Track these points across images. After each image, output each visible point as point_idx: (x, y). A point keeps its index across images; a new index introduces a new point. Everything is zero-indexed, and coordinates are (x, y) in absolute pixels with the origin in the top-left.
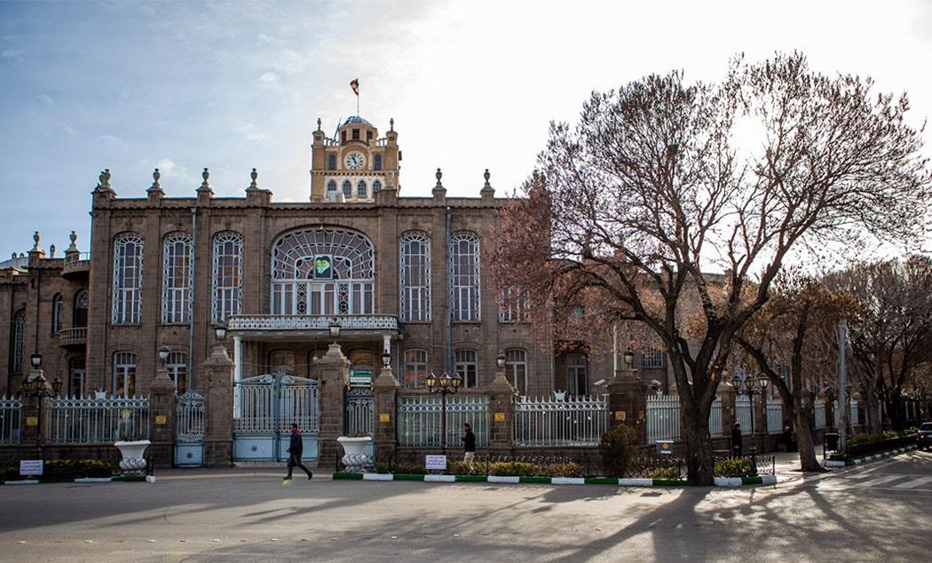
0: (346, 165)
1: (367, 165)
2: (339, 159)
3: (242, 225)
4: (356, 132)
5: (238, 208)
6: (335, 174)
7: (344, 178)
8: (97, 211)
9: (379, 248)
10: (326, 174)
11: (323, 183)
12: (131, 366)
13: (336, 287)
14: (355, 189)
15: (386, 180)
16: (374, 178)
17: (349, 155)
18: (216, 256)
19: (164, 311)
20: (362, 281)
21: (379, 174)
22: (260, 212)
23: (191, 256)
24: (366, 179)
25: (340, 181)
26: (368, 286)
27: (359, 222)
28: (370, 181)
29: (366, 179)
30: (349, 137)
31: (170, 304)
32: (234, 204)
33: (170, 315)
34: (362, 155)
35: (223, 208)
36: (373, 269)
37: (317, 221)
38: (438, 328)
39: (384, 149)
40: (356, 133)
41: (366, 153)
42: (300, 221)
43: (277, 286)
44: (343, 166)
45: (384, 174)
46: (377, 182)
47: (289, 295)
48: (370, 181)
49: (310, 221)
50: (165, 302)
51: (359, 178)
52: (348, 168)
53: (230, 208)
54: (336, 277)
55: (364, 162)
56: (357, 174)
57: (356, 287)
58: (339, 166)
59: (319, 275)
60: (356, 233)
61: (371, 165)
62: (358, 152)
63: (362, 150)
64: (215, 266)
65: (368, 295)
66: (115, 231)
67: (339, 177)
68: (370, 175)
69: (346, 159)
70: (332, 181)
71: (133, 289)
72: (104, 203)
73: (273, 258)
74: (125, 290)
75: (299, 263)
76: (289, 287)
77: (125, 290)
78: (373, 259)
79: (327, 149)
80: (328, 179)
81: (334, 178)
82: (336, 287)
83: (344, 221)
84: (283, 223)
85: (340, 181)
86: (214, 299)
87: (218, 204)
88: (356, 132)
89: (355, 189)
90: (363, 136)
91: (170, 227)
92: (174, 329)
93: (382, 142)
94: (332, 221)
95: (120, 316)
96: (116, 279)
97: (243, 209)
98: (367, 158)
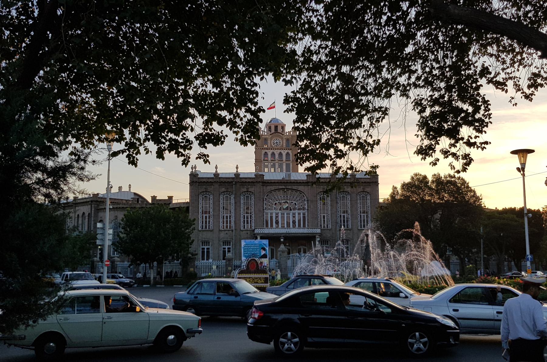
1: (283, 144)
2: (269, 142)
3: (253, 189)
4: (276, 127)
5: (252, 182)
7: (272, 151)
8: (192, 183)
9: (309, 198)
12: (208, 247)
13: (291, 214)
14: (277, 156)
16: (286, 151)
17: (273, 139)
18: (242, 202)
19: (221, 224)
20: (301, 212)
22: (261, 184)
23: (233, 201)
24: (282, 151)
25: (270, 153)
26: (304, 214)
27: (301, 188)
28: (284, 153)
29: (282, 151)
30: (273, 130)
31: (223, 221)
32: (249, 180)
33: (224, 226)
34: (280, 140)
35: (246, 182)
36: (306, 207)
37: (284, 187)
38: (334, 232)
41: (282, 139)
42: (277, 187)
43: (267, 214)
46: (288, 153)
47: (271, 217)
48: (284, 153)
49: (281, 187)
50: (221, 220)
51: (279, 151)
52: (273, 146)
53: (249, 182)
54: (291, 210)
57: (299, 214)
59: (283, 209)
60: (299, 192)
62: (278, 138)
64: (242, 206)
65: (304, 217)
66: (200, 191)
69: (272, 142)
71: (208, 215)
72: (195, 180)
73: (265, 202)
74: (204, 215)
75: (276, 204)
76: (271, 214)
77: (204, 215)
78: (306, 202)
80: (263, 152)
81: (267, 151)
82: (291, 214)
83: (294, 187)
84: (269, 188)
85: (270, 153)
86: (242, 220)
87: (244, 180)
88: (276, 127)
90: (280, 130)
91: (223, 189)
92: (226, 232)
94: (290, 187)
95: (203, 226)
96: (200, 211)
97: (254, 182)
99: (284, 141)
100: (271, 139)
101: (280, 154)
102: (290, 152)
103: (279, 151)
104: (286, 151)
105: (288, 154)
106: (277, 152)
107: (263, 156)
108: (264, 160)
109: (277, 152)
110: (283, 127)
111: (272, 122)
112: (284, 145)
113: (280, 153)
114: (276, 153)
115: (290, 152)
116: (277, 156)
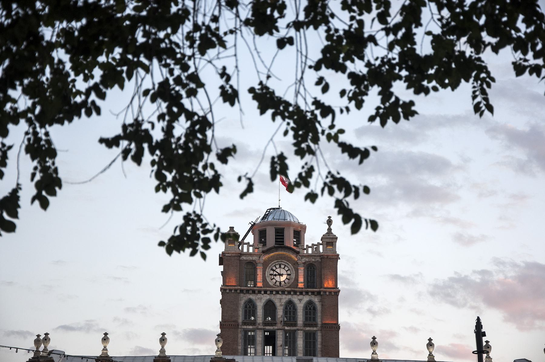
0: (268, 280)
1: (297, 280)
2: (259, 272)
4: (280, 233)
7: (266, 297)
10: (242, 291)
11: (237, 305)
14: (280, 313)
15: (320, 301)
16: (306, 299)
21: (313, 293)
24: (295, 299)
25: (260, 302)
29: (295, 299)
30: (271, 241)
39: (318, 259)
41: (296, 265)
44: (264, 280)
45: (319, 293)
46: (310, 303)
51: (285, 298)
55: (293, 276)
67: (259, 296)
68: (301, 293)
70: (250, 301)
80: (244, 298)
81: (252, 297)
85: (260, 302)
99: (301, 271)
100: (265, 265)
101: (290, 307)
102: (316, 300)
103: (285, 298)
104: (306, 299)
105: (310, 308)
106: (280, 301)
107: (241, 313)
108: (244, 323)
109: (280, 301)
111: (270, 218)
112: (301, 279)
113: (290, 303)
114: (278, 304)
115: (316, 300)
116: (280, 313)
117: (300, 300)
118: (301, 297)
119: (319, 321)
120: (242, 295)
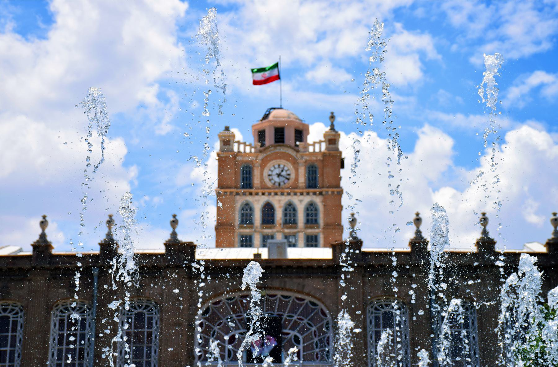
0: (266, 180)
1: (297, 179)
2: (256, 173)
6: (251, 194)
10: (237, 194)
11: (233, 207)
14: (279, 215)
15: (323, 201)
16: (307, 199)
17: (270, 165)
21: (314, 194)
24: (295, 200)
25: (258, 204)
28: (301, 203)
29: (295, 200)
30: (269, 139)
39: (320, 157)
40: (281, 136)
41: (295, 163)
45: (321, 193)
48: (301, 203)
51: (285, 199)
55: (293, 176)
56: (282, 194)
58: (256, 181)
61: (302, 180)
63: (287, 157)
67: (257, 197)
68: (302, 194)
69: (266, 172)
79: (239, 158)
80: (240, 201)
81: (249, 199)
89: (301, 218)
93: (317, 146)
98: (297, 170)
99: (302, 171)
100: (263, 165)
102: (318, 200)
103: (285, 199)
105: (311, 209)
108: (241, 227)
109: (279, 203)
110: (300, 134)
115: (318, 200)
117: (301, 201)
118: (301, 197)
119: (321, 222)
120: (238, 197)
